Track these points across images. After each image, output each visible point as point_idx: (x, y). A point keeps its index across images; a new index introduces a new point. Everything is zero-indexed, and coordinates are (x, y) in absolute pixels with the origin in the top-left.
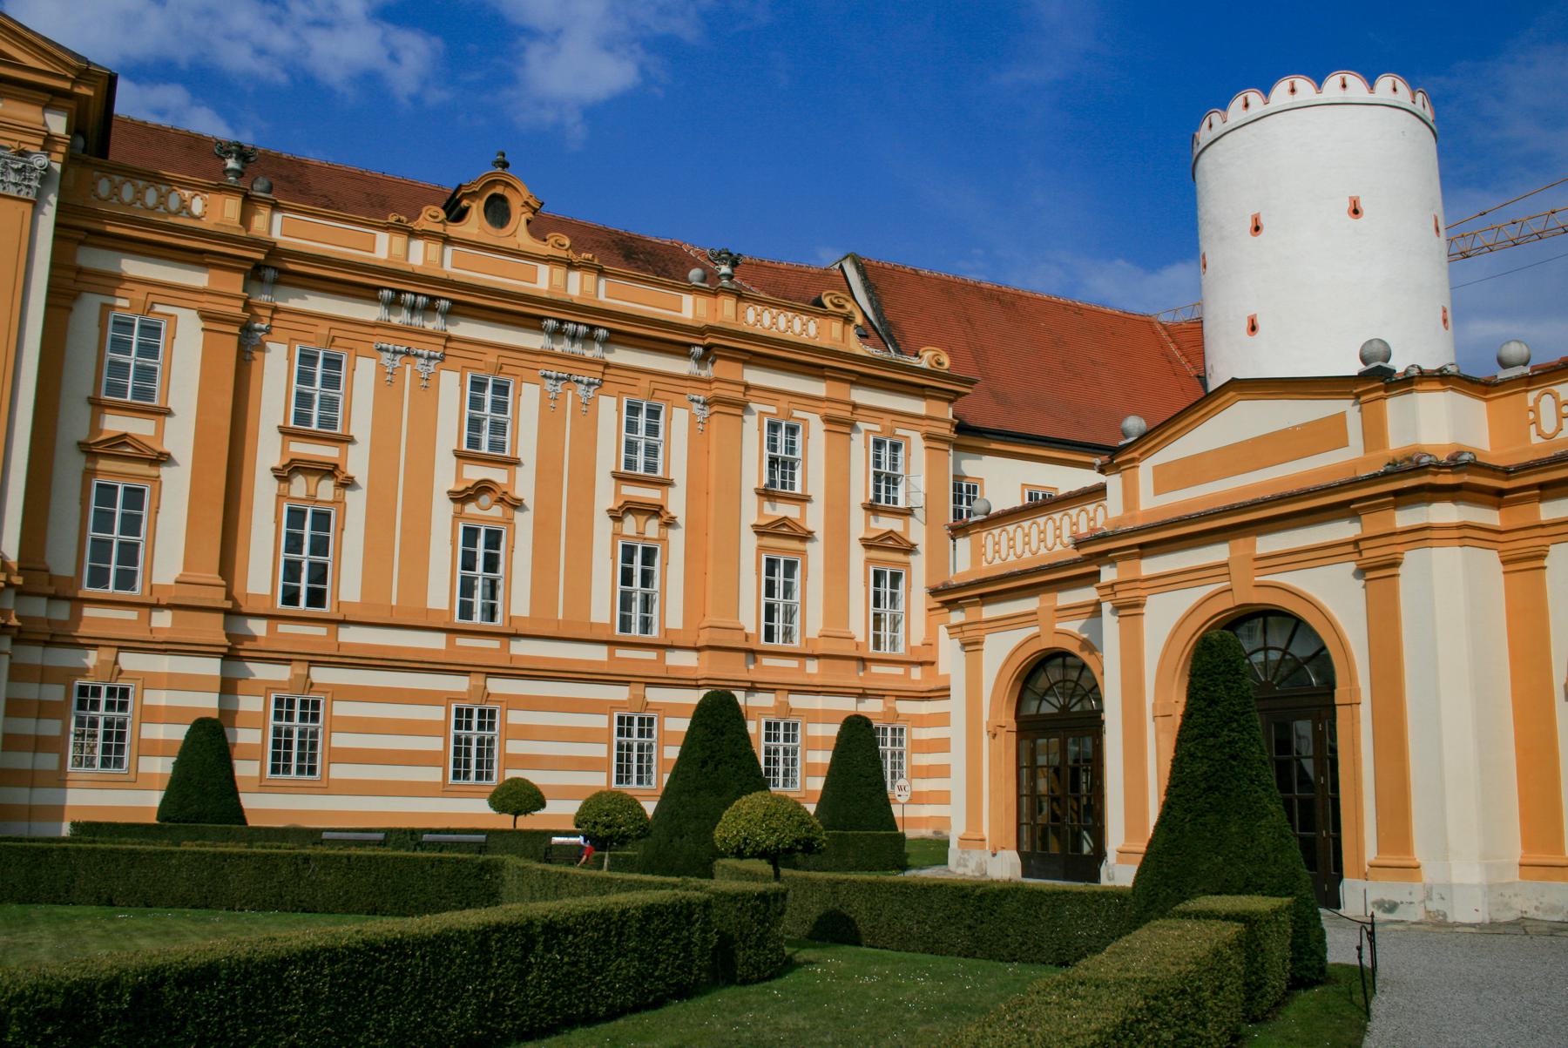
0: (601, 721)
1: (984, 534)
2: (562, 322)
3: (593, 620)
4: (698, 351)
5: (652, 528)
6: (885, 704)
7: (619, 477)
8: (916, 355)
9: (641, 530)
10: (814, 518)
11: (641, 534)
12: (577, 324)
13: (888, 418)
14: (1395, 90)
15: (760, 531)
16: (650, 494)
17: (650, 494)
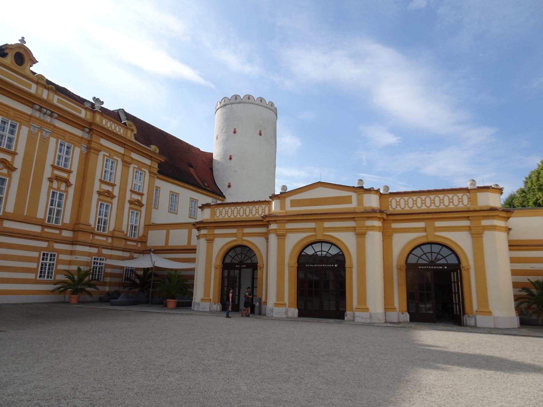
0: (36, 254)
1: (216, 209)
2: (41, 107)
3: (37, 217)
4: (87, 130)
5: (63, 186)
6: (130, 254)
7: (53, 167)
8: (150, 147)
9: (59, 187)
10: (116, 192)
11: (59, 189)
12: (46, 109)
13: (140, 165)
14: (272, 106)
15: (100, 193)
16: (65, 175)
17: (65, 175)
